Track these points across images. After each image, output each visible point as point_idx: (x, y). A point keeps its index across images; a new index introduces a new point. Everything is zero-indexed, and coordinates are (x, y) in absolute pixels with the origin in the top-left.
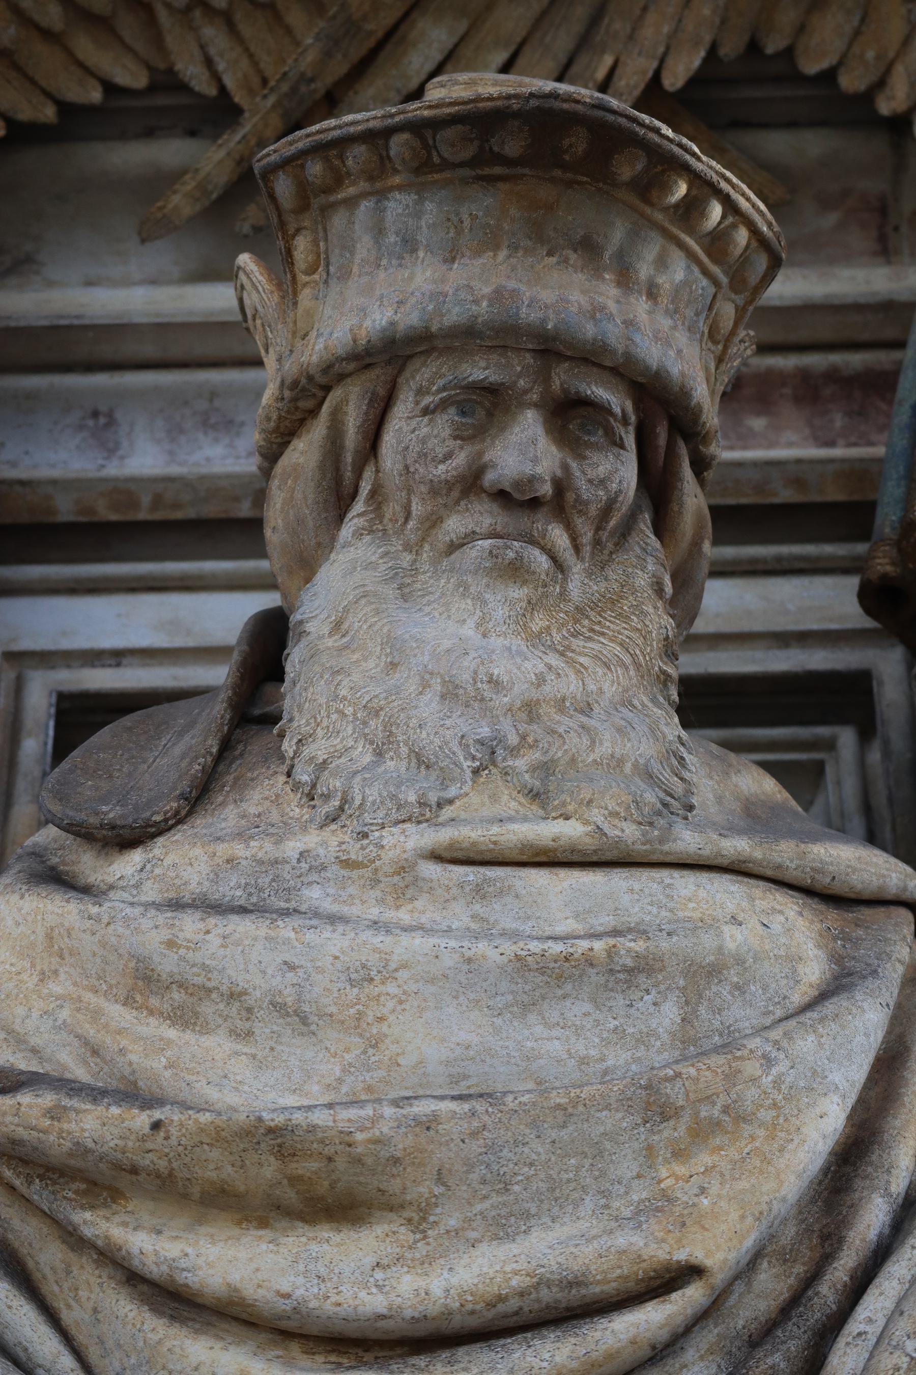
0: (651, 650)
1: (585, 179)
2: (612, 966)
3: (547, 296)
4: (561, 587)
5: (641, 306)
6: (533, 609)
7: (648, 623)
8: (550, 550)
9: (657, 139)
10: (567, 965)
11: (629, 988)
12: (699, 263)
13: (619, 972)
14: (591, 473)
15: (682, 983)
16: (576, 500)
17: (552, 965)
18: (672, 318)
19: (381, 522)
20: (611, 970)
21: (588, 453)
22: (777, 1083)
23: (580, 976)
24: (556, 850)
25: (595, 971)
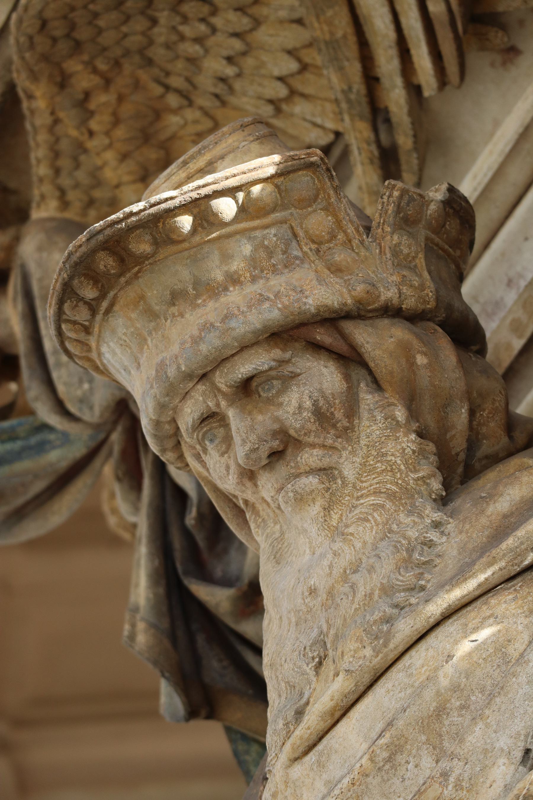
0: (401, 474)
1: (136, 269)
2: (378, 766)
3: (175, 348)
4: (341, 478)
5: (234, 297)
6: (329, 511)
7: (389, 458)
8: (311, 469)
9: (134, 219)
10: (355, 787)
11: (396, 770)
12: (255, 229)
13: (384, 766)
14: (291, 409)
15: (424, 738)
16: (296, 432)
17: (349, 794)
18: (262, 278)
19: (259, 517)
20: (379, 769)
21: (281, 400)
22: (458, 786)
23: (367, 787)
24: (337, 703)
25: (371, 777)
